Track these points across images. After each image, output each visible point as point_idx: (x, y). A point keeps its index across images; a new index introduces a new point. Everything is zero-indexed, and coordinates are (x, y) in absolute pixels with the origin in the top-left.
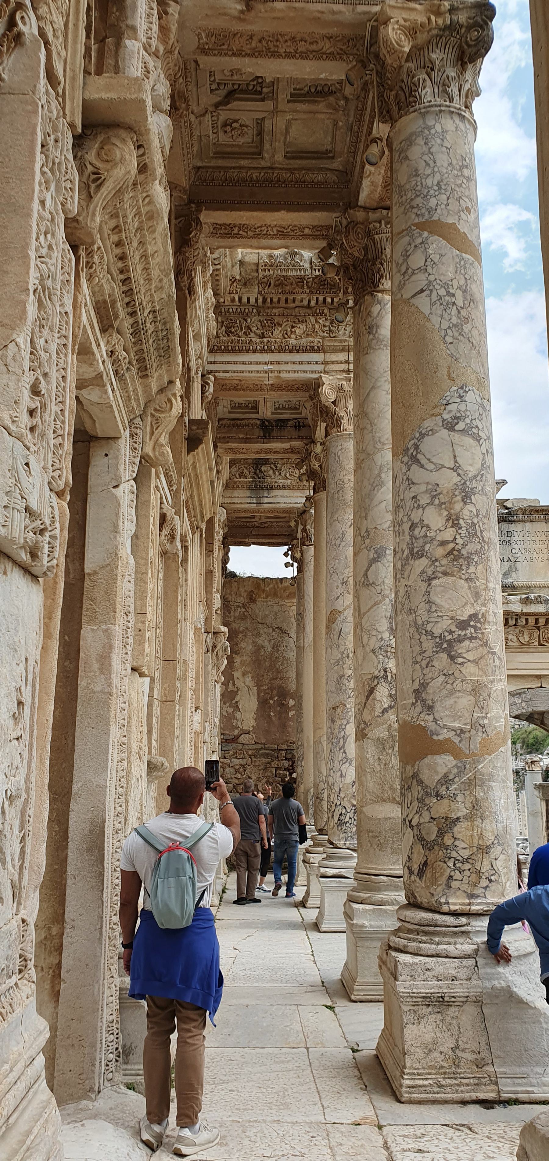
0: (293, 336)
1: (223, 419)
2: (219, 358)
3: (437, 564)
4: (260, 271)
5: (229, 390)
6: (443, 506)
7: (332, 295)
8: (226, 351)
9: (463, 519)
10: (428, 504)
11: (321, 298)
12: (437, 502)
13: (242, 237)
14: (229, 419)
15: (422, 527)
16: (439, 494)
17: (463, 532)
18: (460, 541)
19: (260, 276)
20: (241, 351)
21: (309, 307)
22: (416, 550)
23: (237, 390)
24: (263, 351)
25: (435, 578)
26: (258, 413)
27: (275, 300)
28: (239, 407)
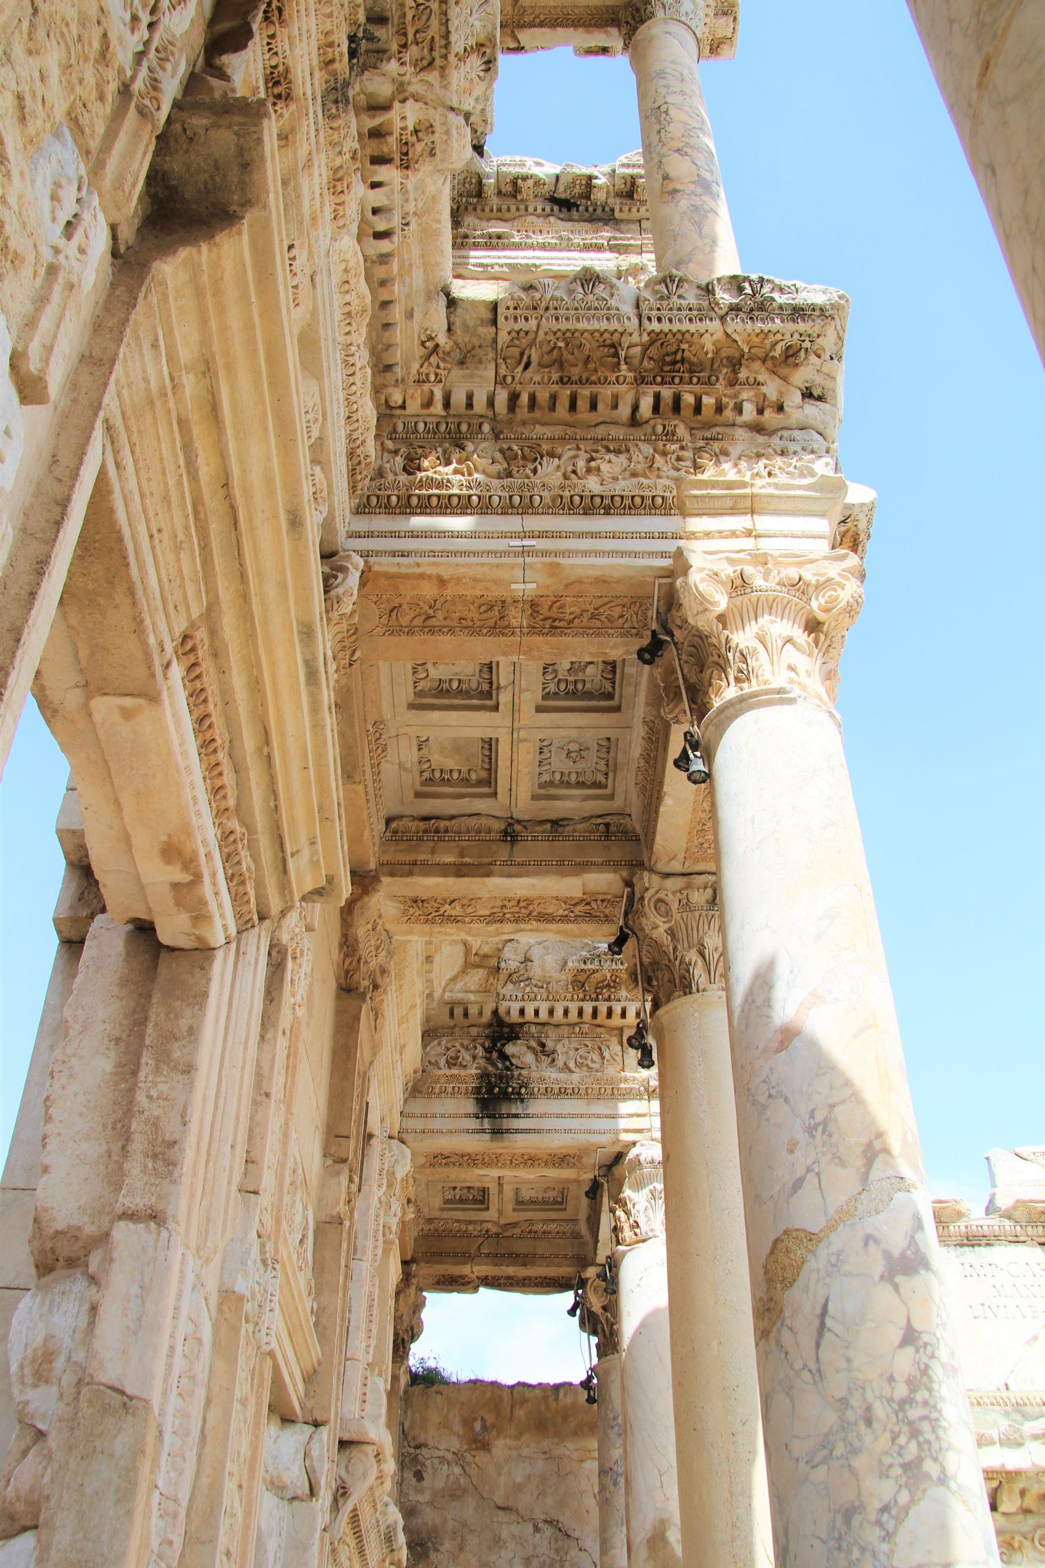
1: (401, 817)
2: (381, 523)
4: (501, 320)
5: (411, 632)
7: (698, 389)
11: (667, 393)
19: (503, 338)
21: (634, 421)
23: (432, 631)
27: (543, 396)
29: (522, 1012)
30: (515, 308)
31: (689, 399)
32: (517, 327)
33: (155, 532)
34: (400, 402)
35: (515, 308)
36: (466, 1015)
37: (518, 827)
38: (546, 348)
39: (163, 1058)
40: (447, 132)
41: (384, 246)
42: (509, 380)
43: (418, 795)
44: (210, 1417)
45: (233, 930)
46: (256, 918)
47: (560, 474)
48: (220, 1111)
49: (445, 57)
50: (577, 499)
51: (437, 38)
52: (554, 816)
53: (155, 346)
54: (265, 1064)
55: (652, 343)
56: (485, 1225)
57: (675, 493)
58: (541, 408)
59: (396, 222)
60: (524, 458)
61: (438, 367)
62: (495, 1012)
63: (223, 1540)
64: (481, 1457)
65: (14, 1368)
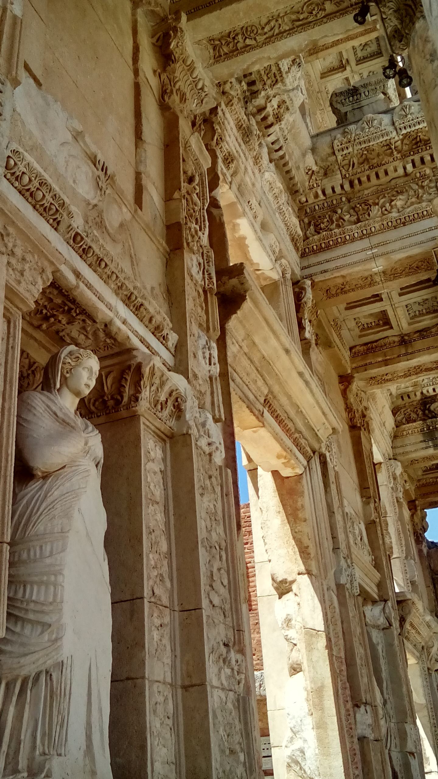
0: (395, 210)
1: (356, 346)
2: (313, 259)
4: (336, 152)
5: (337, 295)
8: (321, 250)
11: (417, 158)
13: (251, 48)
14: (361, 345)
19: (340, 158)
20: (337, 244)
21: (406, 175)
23: (345, 292)
26: (392, 328)
27: (364, 179)
28: (369, 328)
30: (341, 145)
31: (428, 158)
32: (345, 152)
33: (248, 384)
34: (305, 200)
35: (341, 145)
38: (359, 156)
40: (291, 100)
41: (281, 153)
42: (347, 176)
43: (360, 336)
45: (305, 463)
46: (312, 455)
47: (380, 212)
48: (319, 529)
49: (282, 76)
50: (390, 224)
51: (276, 72)
53: (233, 343)
54: (329, 501)
55: (405, 138)
57: (431, 207)
60: (363, 209)
61: (316, 180)
62: (422, 393)
63: (358, 661)
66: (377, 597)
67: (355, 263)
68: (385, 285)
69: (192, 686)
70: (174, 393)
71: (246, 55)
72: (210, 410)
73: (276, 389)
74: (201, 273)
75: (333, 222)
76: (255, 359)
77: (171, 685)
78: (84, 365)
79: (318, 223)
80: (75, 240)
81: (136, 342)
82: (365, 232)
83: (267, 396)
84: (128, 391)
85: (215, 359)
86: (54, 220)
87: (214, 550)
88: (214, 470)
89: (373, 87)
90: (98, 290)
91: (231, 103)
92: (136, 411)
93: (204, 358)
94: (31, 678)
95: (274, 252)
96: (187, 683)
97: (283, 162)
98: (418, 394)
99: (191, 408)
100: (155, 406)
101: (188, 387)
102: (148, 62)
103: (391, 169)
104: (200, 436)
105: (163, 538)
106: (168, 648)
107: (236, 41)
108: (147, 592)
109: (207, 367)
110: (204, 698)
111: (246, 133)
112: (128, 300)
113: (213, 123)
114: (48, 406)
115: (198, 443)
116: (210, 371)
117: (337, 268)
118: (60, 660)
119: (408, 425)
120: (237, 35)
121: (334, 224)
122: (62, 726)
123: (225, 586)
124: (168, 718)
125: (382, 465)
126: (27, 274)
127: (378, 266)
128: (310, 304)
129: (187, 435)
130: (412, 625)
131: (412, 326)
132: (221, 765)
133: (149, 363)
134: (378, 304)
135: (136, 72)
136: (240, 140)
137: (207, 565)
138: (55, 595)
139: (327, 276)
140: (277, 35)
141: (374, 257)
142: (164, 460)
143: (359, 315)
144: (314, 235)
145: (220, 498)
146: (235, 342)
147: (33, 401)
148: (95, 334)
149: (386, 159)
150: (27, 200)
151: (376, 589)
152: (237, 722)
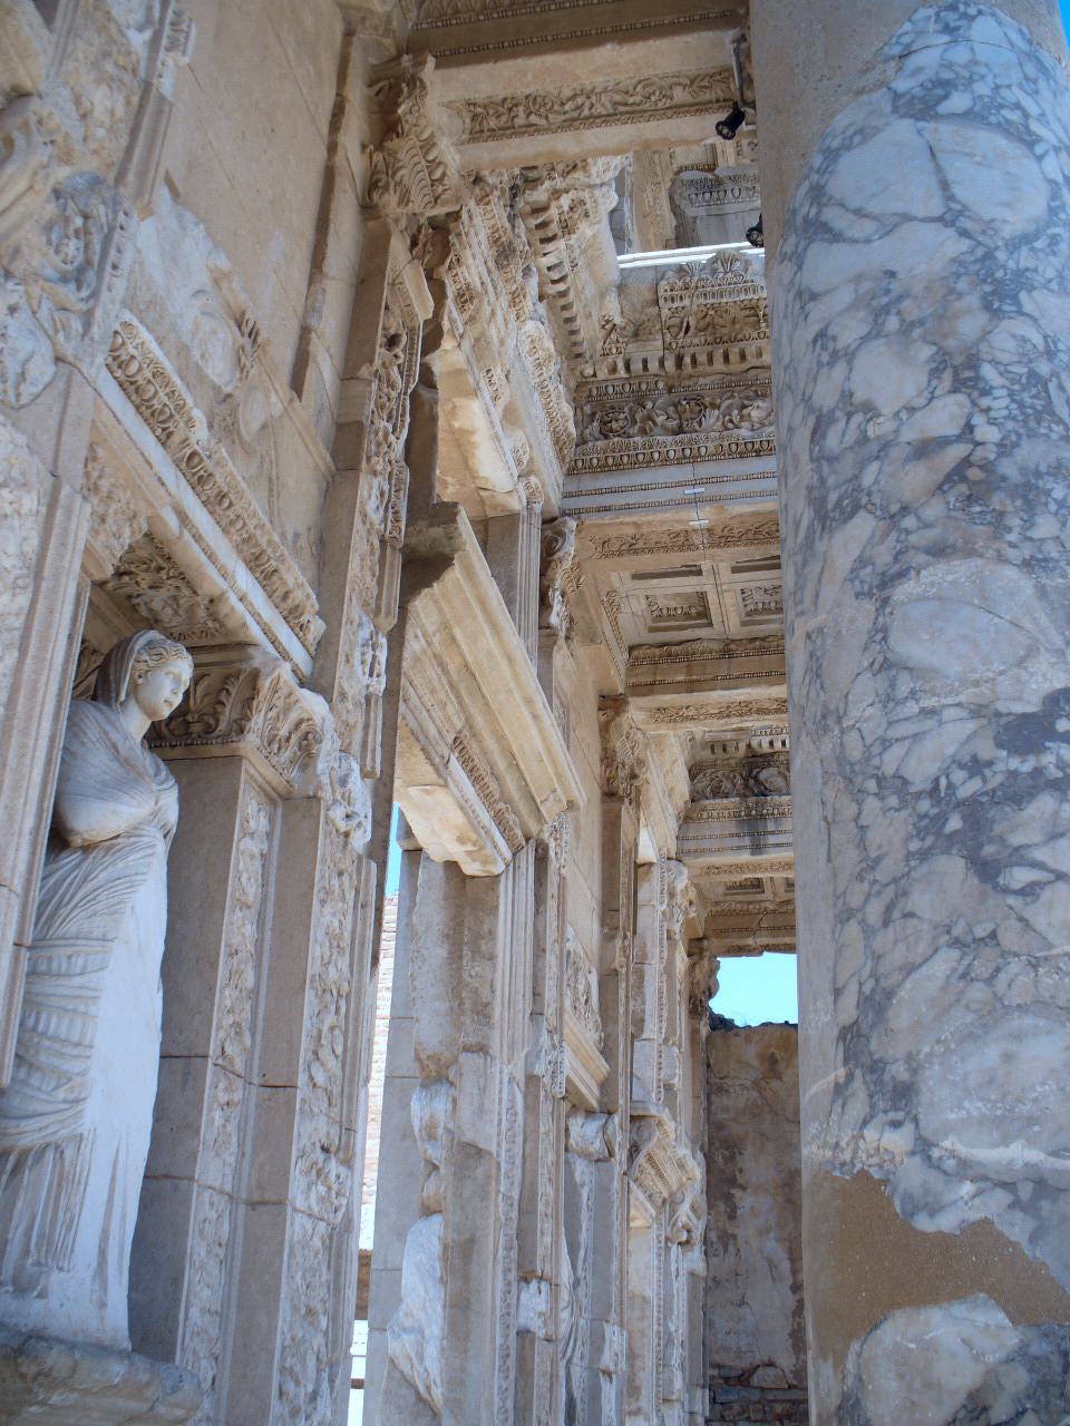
0: (746, 424)
1: (640, 646)
2: (589, 483)
3: (909, 522)
4: (661, 302)
5: (620, 554)
6: (917, 332)
8: (604, 468)
9: (995, 362)
10: (864, 339)
12: (892, 323)
13: (538, 130)
15: (849, 415)
16: (900, 298)
17: (1000, 404)
18: (988, 433)
19: (665, 312)
20: (634, 464)
22: (833, 498)
23: (636, 552)
24: (679, 462)
25: (902, 574)
26: (710, 624)
27: (702, 358)
29: (771, 743)
36: (724, 750)
37: (733, 646)
38: (700, 315)
39: (476, 951)
40: (595, 201)
41: (561, 287)
42: (674, 345)
43: (652, 630)
44: (527, 1149)
45: (509, 856)
47: (719, 423)
50: (734, 447)
52: (761, 635)
53: (416, 637)
54: (540, 929)
56: (763, 905)
58: (702, 364)
59: (567, 268)
60: (692, 411)
62: (749, 746)
63: (541, 1207)
64: (775, 1084)
65: (416, 1130)
66: (595, 1104)
67: (661, 504)
68: (708, 552)
69: (263, 1203)
70: (303, 726)
71: (526, 139)
72: (358, 755)
73: (480, 721)
74: (382, 512)
75: (634, 422)
76: (452, 668)
77: (231, 1197)
78: (170, 668)
79: (606, 419)
80: (193, 467)
81: (255, 632)
82: (688, 452)
83: (460, 732)
84: (228, 714)
85: (381, 667)
86: (164, 430)
87: (328, 996)
88: (348, 862)
89: (749, 185)
90: (211, 543)
91: (486, 200)
92: (239, 749)
93: (363, 663)
94: (33, 1153)
95: (519, 462)
96: (256, 1198)
97: (562, 302)
98: (742, 746)
99: (327, 749)
100: (269, 744)
101: (329, 716)
102: (356, 127)
103: (751, 349)
104: (335, 801)
105: (250, 966)
106: (234, 1139)
107: (512, 114)
108: (213, 1050)
109: (366, 680)
110: (279, 1224)
111: (504, 253)
112: (255, 562)
113: (448, 232)
114: (106, 733)
115: (331, 813)
116: (368, 686)
117: (628, 507)
118: (80, 1130)
119: (712, 802)
120: (516, 105)
121: (636, 427)
122: (69, 1228)
123: (337, 1057)
124: (220, 1245)
125: (654, 869)
126: (110, 520)
127: (700, 518)
128: (568, 564)
129: (315, 798)
130: (650, 1159)
131: (746, 629)
132: (291, 1327)
133: (272, 672)
134: (693, 580)
135: (332, 148)
136: (491, 264)
137: (314, 1020)
138: (83, 1033)
139: (607, 518)
140: (587, 118)
141: (696, 501)
142: (269, 835)
143: (657, 592)
144: (596, 439)
145: (351, 910)
146: (420, 634)
147: (82, 720)
148: (191, 609)
149: (748, 331)
150: (129, 397)
151: (596, 1091)
152: (324, 1269)
